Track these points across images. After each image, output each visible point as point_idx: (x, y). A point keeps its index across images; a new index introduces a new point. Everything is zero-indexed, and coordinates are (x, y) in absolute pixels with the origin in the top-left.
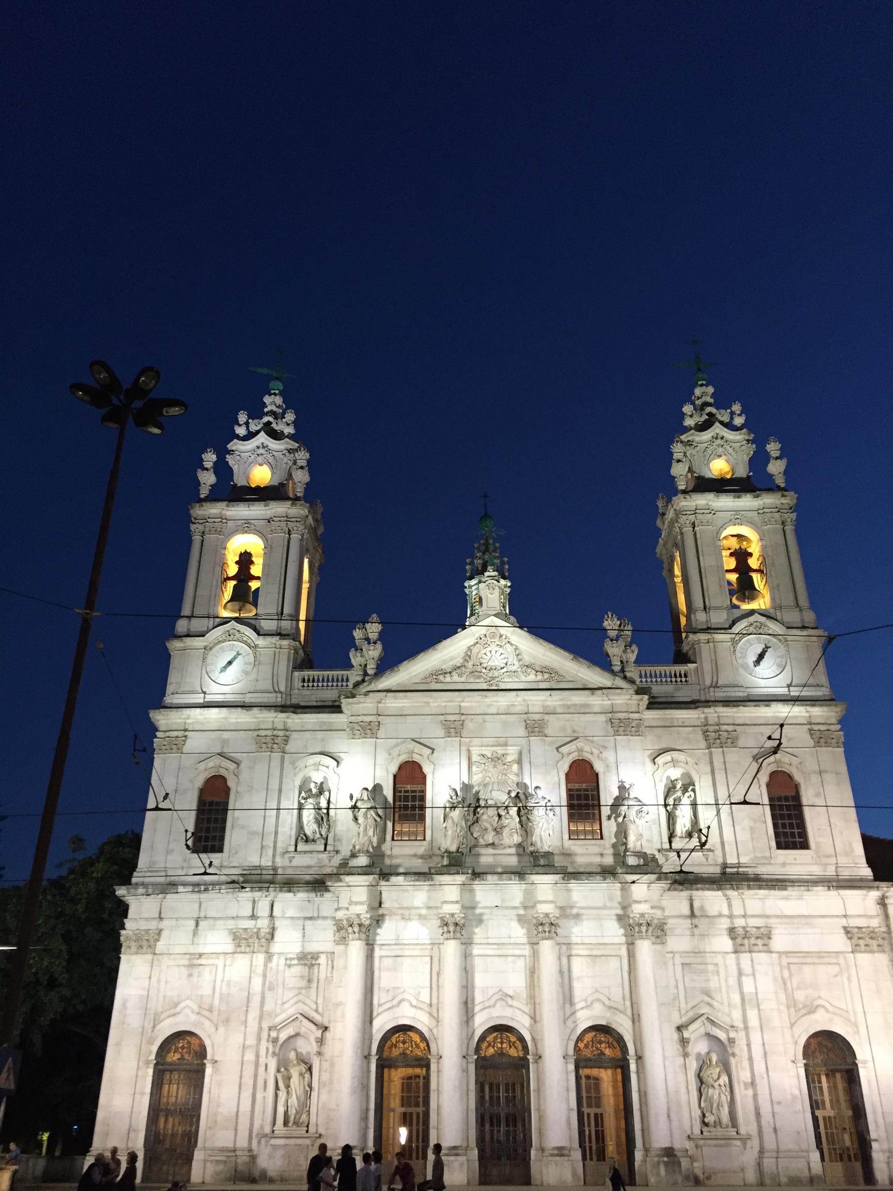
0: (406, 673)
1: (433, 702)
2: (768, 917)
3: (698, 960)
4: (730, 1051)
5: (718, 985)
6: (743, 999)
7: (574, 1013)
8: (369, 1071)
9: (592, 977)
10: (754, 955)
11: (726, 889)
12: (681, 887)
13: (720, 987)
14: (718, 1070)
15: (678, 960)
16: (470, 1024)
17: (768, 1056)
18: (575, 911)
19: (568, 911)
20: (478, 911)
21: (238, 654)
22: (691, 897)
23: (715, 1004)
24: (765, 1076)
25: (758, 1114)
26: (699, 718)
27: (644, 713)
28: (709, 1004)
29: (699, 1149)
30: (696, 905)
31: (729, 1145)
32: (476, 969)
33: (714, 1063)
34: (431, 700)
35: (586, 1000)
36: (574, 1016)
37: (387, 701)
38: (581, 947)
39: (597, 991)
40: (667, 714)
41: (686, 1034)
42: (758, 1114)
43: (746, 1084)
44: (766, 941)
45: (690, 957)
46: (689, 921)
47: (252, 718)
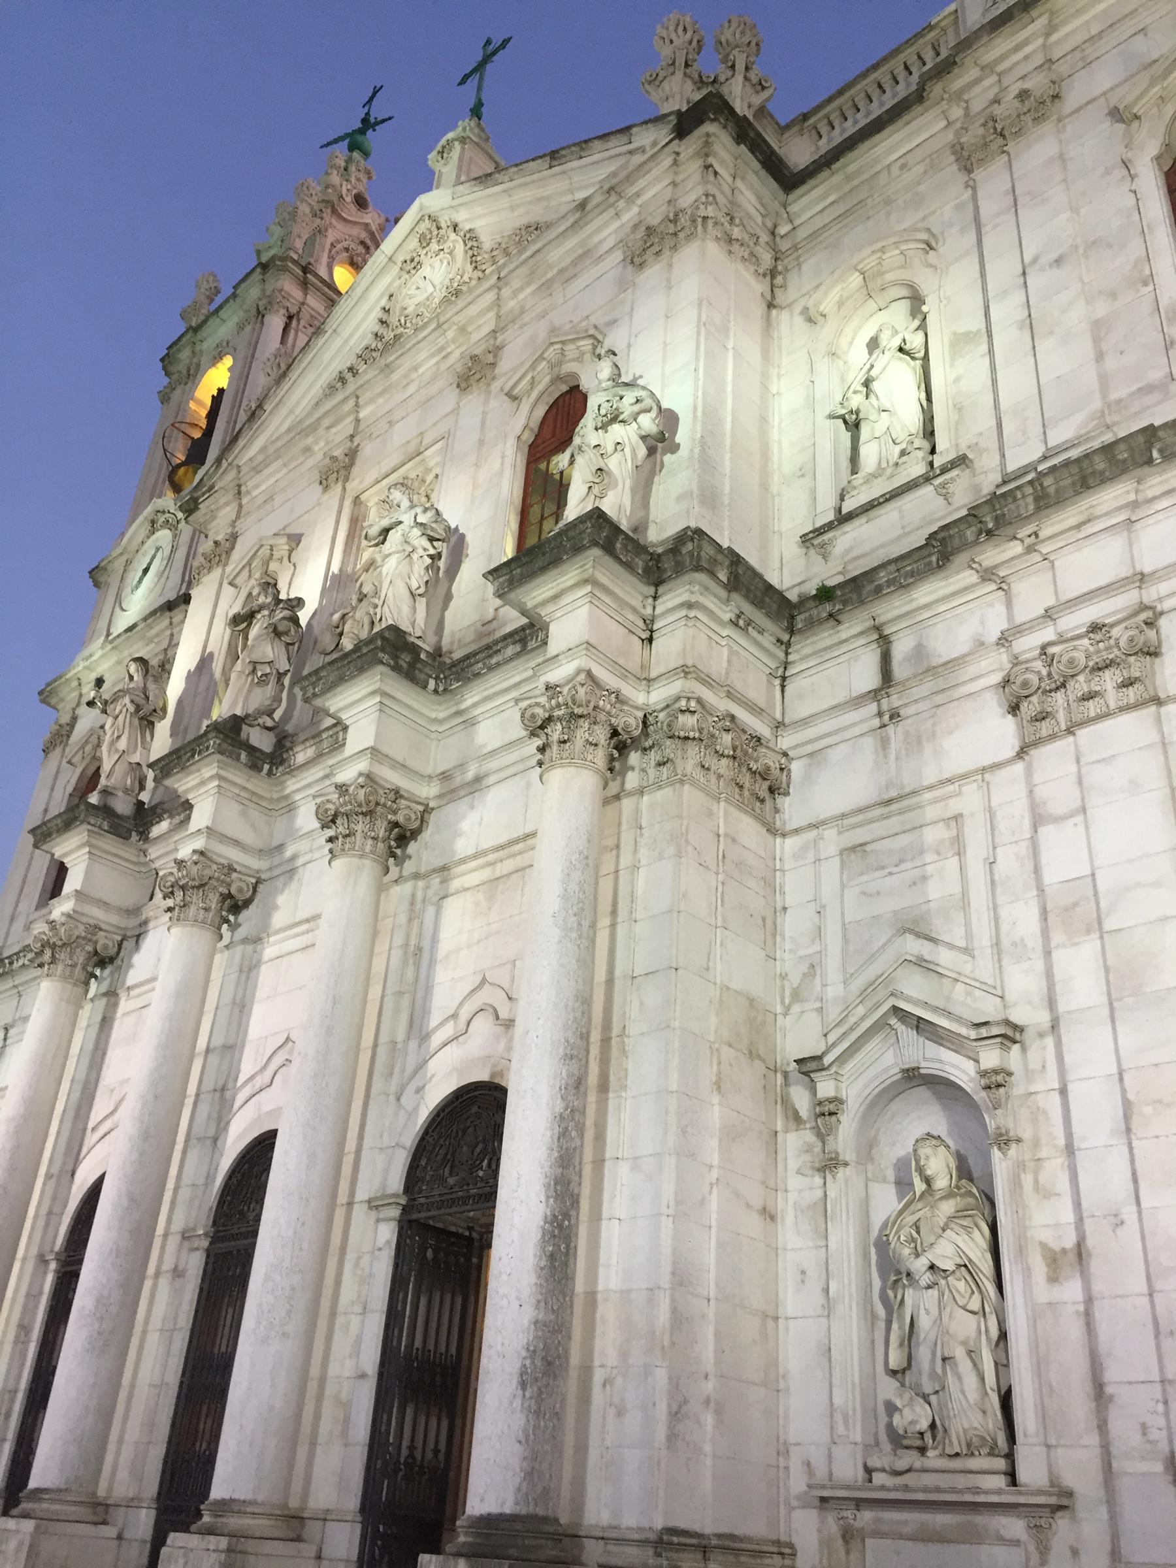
0: (283, 411)
1: (316, 442)
2: (1142, 579)
3: (894, 823)
4: (991, 1124)
5: (957, 890)
6: (1044, 914)
7: (422, 1065)
8: (41, 1293)
9: (479, 942)
10: (1083, 733)
11: (965, 546)
12: (828, 607)
13: (965, 894)
14: (948, 1208)
15: (832, 841)
16: (219, 1143)
17: (1135, 1123)
18: (470, 775)
19: (458, 780)
20: (288, 853)
21: (158, 549)
22: (877, 628)
23: (945, 958)
24: (1129, 1212)
25: (1100, 1393)
26: (949, 124)
27: (794, 208)
28: (922, 964)
29: (855, 1545)
30: (901, 648)
31: (974, 1537)
32: (260, 994)
33: (941, 1183)
34: (310, 440)
35: (455, 1016)
36: (421, 1073)
37: (250, 484)
38: (473, 864)
39: (484, 981)
40: (858, 172)
41: (826, 1088)
42: (1100, 1393)
43: (1054, 1260)
44: (1136, 667)
45: (871, 821)
46: (873, 708)
47: (147, 645)
